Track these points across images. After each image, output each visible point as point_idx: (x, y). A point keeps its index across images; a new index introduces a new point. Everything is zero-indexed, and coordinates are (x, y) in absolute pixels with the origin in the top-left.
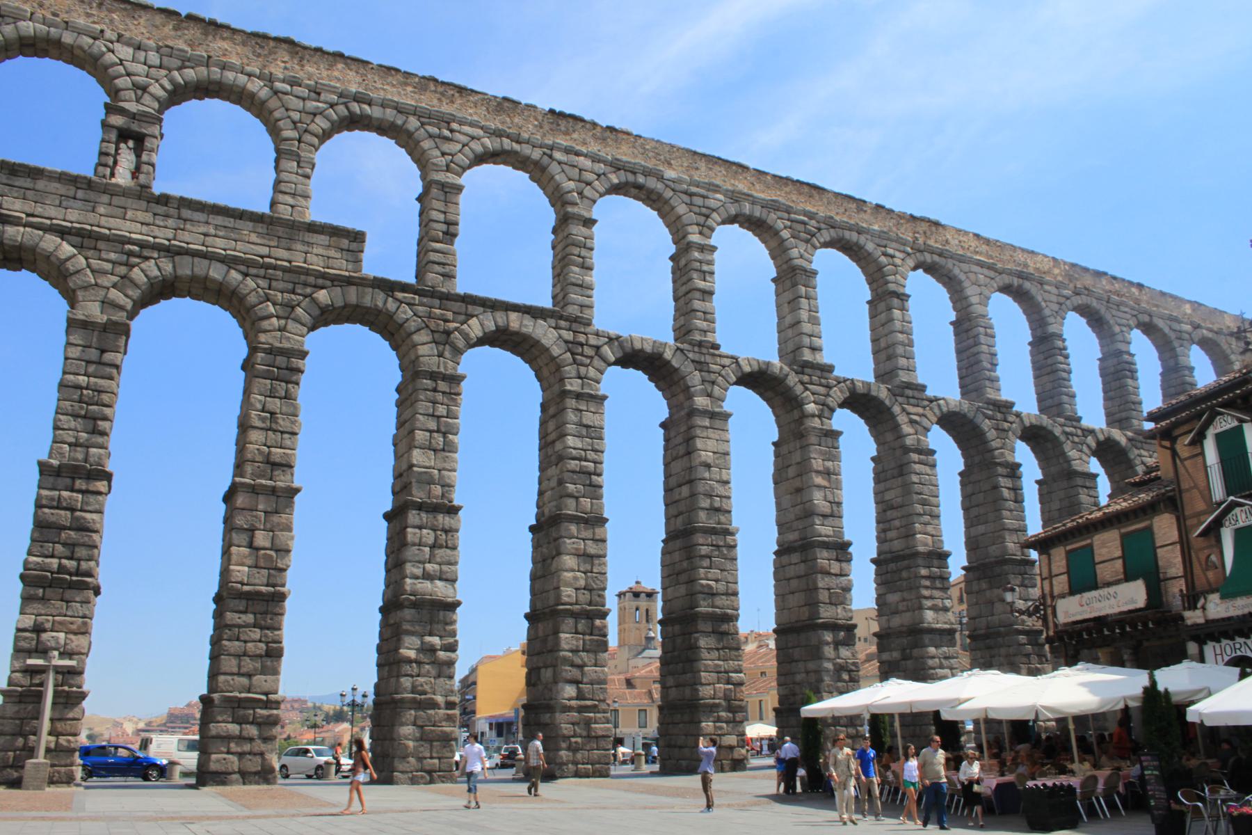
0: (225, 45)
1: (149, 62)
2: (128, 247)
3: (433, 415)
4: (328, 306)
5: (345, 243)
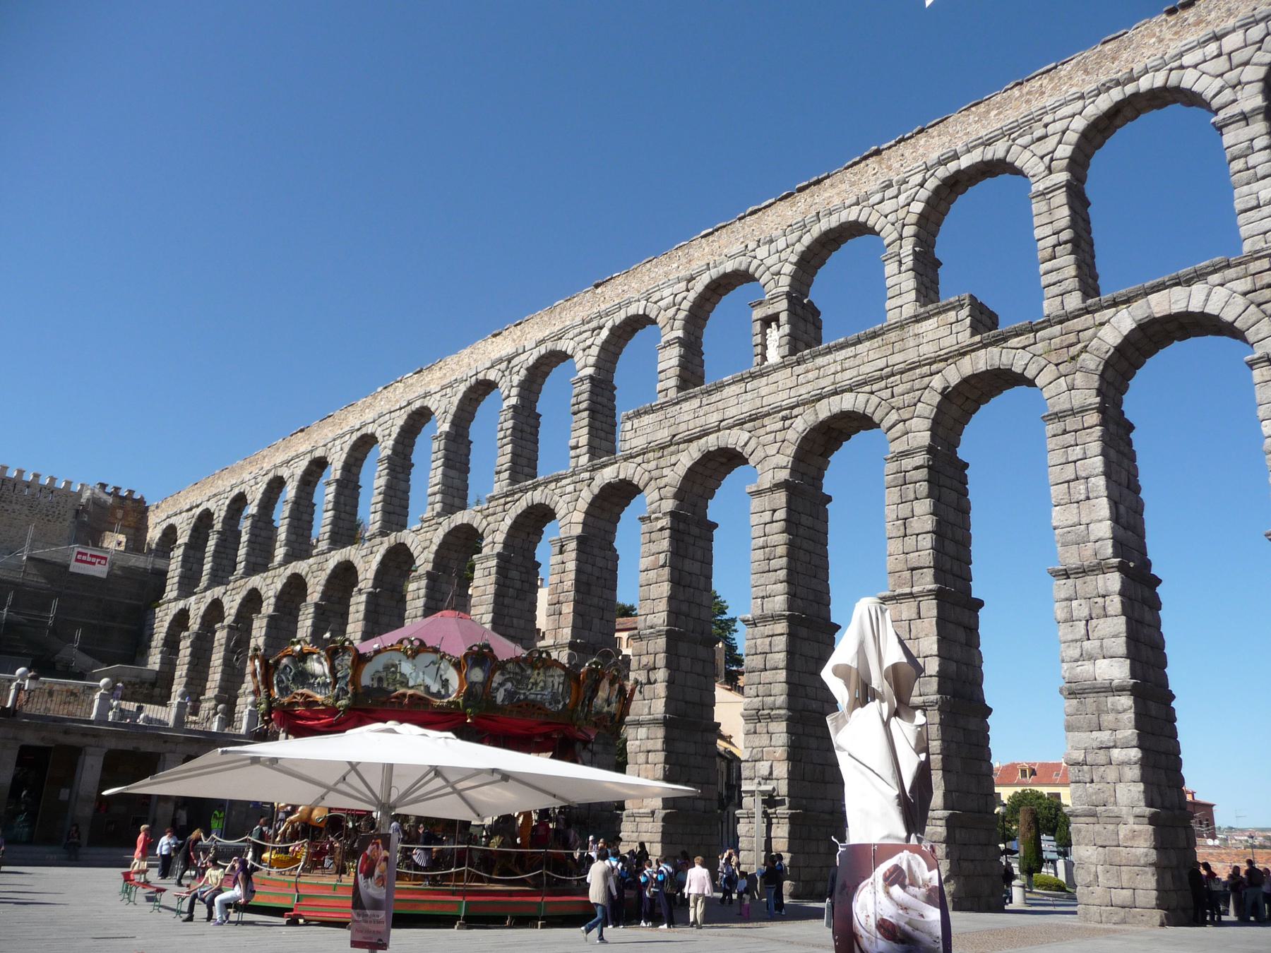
0: (830, 192)
4: (945, 389)
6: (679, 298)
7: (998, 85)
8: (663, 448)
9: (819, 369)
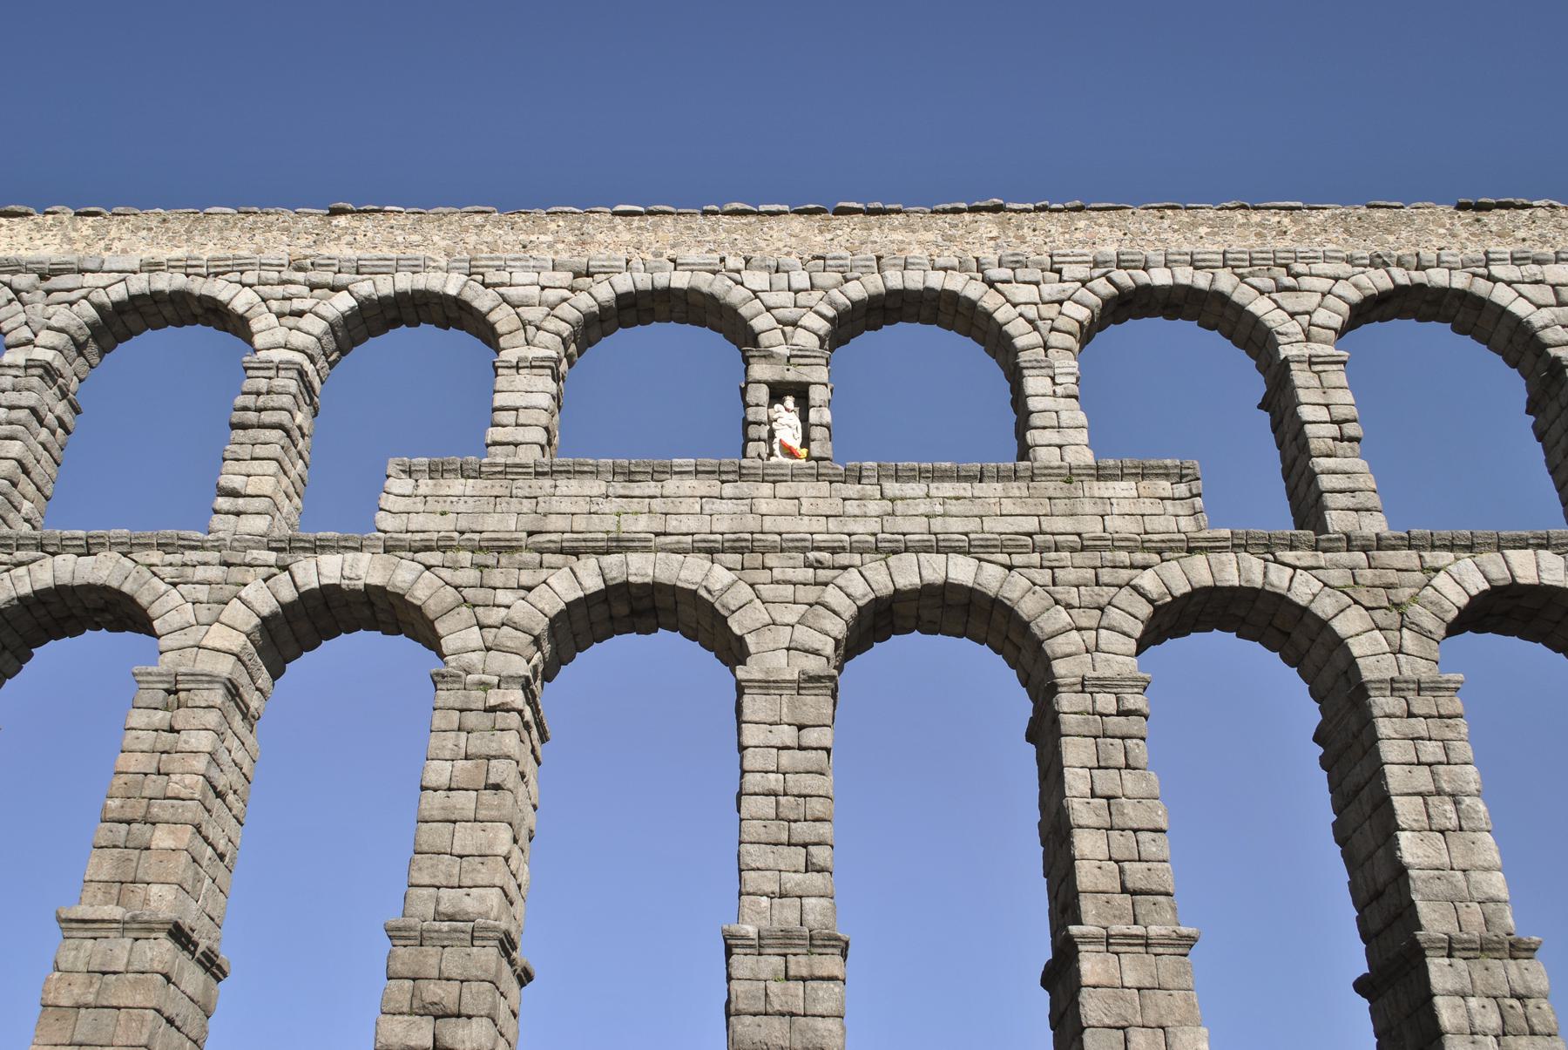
1: (795, 285)
2: (812, 555)
3: (1419, 764)
4: (1162, 596)
5: (1164, 487)
6: (552, 295)
7: (1216, 198)
8: (500, 549)
9: (892, 500)
